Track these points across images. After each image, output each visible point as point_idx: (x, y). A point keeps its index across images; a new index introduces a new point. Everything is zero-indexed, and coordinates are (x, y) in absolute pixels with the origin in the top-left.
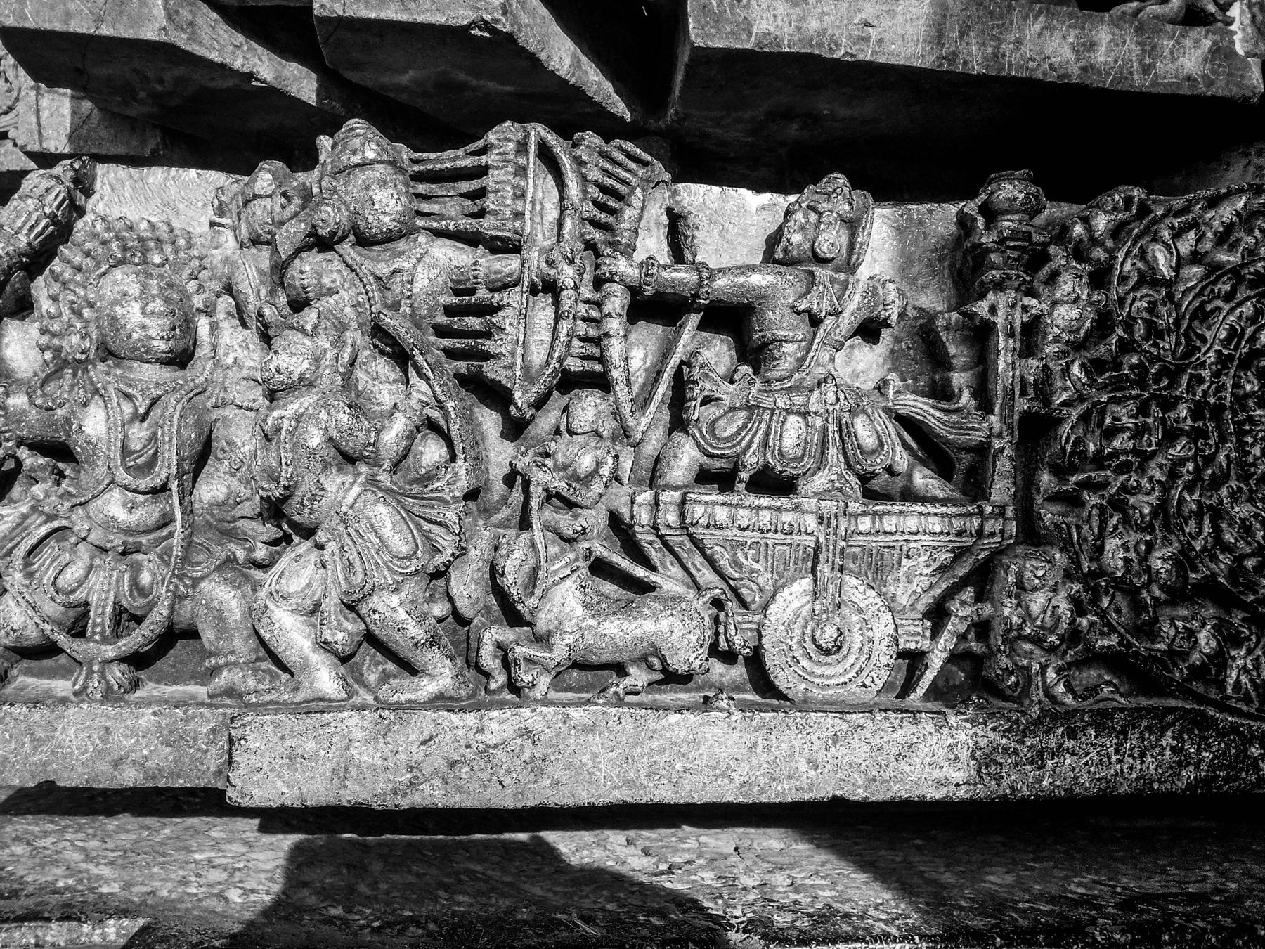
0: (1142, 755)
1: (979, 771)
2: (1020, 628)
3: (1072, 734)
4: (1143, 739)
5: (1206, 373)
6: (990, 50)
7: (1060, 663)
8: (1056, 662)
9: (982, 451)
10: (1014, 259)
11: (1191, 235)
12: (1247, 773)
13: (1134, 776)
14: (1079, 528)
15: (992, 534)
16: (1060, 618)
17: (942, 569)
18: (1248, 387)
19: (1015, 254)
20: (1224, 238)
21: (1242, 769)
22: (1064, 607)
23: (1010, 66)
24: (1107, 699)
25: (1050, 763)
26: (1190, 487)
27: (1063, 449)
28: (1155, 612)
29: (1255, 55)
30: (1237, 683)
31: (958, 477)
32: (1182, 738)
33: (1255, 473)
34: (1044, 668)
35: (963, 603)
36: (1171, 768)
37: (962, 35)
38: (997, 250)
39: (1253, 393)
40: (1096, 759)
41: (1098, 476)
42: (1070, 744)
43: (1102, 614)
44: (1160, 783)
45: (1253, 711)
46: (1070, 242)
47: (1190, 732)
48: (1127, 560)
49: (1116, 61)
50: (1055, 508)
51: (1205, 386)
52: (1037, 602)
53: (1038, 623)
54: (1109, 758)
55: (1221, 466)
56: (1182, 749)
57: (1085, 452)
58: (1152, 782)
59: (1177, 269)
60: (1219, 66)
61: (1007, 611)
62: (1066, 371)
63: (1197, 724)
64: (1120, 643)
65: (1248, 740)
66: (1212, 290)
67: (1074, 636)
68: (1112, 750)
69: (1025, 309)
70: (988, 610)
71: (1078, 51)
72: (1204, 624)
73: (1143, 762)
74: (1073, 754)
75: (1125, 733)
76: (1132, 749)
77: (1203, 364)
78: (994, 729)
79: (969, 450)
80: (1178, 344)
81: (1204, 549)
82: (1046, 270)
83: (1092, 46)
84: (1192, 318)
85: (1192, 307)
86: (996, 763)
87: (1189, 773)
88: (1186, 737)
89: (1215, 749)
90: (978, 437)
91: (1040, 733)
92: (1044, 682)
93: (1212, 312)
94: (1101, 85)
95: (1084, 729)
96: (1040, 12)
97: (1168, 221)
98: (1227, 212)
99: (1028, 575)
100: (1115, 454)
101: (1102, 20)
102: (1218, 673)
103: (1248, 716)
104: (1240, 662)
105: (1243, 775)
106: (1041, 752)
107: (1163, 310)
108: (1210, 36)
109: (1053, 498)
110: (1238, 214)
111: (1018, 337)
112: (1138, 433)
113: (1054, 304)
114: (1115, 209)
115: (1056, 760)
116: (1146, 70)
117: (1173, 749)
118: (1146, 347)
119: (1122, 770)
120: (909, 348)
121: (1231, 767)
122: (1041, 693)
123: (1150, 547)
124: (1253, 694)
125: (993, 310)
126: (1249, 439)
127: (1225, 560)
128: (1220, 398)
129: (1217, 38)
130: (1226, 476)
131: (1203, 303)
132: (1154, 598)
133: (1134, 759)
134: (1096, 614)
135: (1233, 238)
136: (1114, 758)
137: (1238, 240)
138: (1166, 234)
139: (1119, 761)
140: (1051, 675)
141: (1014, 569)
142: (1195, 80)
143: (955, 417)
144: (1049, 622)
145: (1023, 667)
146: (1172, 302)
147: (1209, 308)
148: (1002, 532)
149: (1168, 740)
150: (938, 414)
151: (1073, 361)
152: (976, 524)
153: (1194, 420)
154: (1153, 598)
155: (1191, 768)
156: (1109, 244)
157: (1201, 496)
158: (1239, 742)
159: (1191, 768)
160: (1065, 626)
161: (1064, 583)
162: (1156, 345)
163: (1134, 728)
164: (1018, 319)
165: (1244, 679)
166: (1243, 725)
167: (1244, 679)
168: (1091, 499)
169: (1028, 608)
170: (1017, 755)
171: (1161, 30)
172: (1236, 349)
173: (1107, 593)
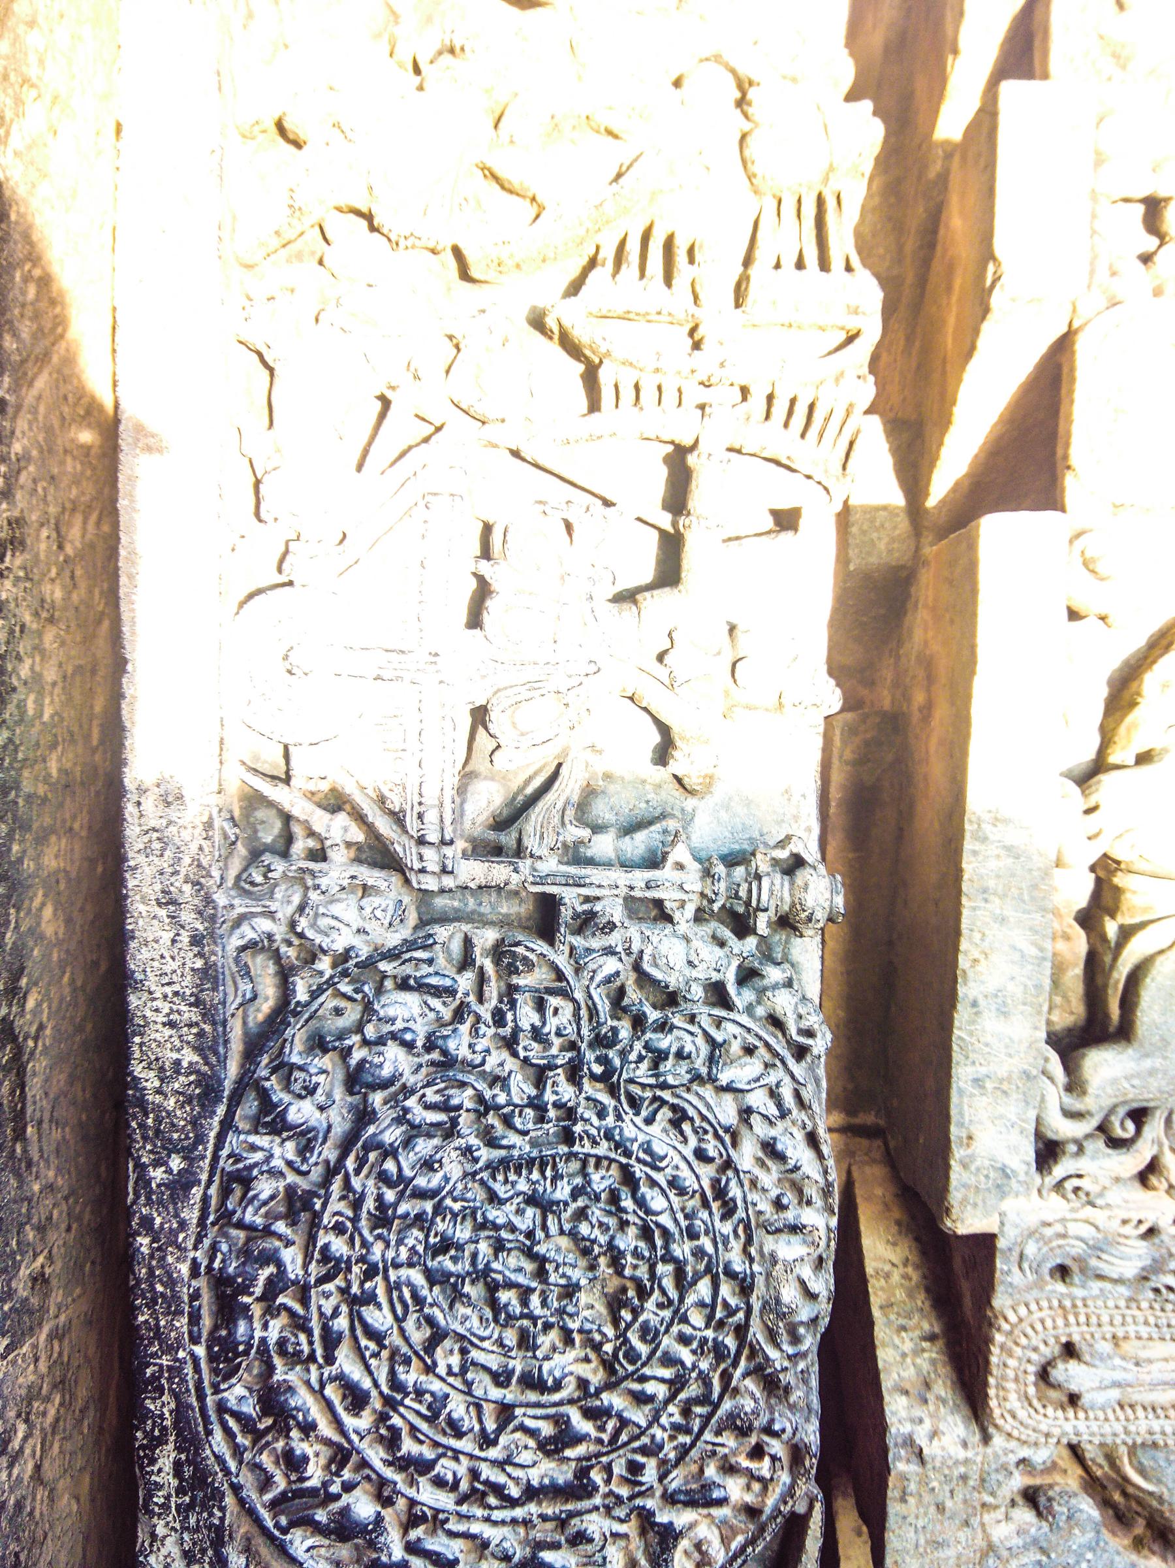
0: (171, 1024)
1: (154, 830)
2: (317, 887)
3: (196, 940)
4: (190, 1026)
5: (610, 1120)
6: (991, 883)
7: (278, 937)
8: (279, 931)
9: (519, 851)
10: (737, 892)
11: (773, 1111)
12: (151, 1152)
13: (148, 1013)
14: (430, 962)
15: (421, 858)
16: (327, 935)
17: (382, 800)
18: (595, 1177)
19: (743, 893)
20: (770, 1149)
21: (155, 1146)
22: (339, 946)
23: (974, 909)
24: (236, 990)
25: (162, 913)
26: (480, 1098)
27: (518, 944)
28: (335, 1049)
29: (1002, 1223)
30: (253, 1148)
31: (492, 835)
32: (191, 1073)
33: (495, 1179)
34: (271, 915)
35: (346, 830)
36: (157, 1059)
37: (1008, 849)
38: (748, 874)
39: (589, 1183)
40: (167, 969)
41: (493, 990)
42: (185, 938)
43: (330, 983)
44: (141, 1045)
45: (221, 1163)
46: (761, 963)
47: (198, 1083)
48: (393, 1020)
49: (987, 1045)
50: (456, 946)
51: (595, 1121)
52: (347, 909)
53: (321, 910)
54: (169, 984)
55: (503, 1137)
56: (178, 1072)
57: (517, 972)
58: (142, 1035)
59: (729, 1089)
60: (987, 1177)
61: (334, 874)
62: (609, 951)
63: (208, 1090)
64: (298, 1003)
65: (189, 1155)
66: (706, 1132)
67: (311, 955)
68: (176, 988)
69: (682, 904)
70: (339, 856)
71: (996, 996)
72: (322, 1109)
73: (164, 1024)
74: (174, 941)
75: (196, 1004)
76: (179, 1012)
77: (619, 1117)
78: (201, 849)
79: (519, 841)
80: (643, 1086)
81: (406, 1111)
82: (726, 933)
83: (1003, 1013)
84: (674, 1108)
85: (686, 1106)
86: (163, 850)
87: (151, 1081)
88: (192, 1078)
89: (178, 1113)
90: (531, 843)
91: (196, 902)
92: (254, 915)
93: (682, 1133)
94: (956, 1023)
95: (200, 955)
96: (1041, 949)
97: (787, 1079)
98: (798, 1152)
99: (376, 901)
100: (513, 1004)
101: (1036, 1028)
102: (266, 1125)
103: (216, 1158)
104: (277, 1151)
105: (149, 1147)
106: (173, 902)
107: (684, 1066)
108: (1024, 1167)
109: (468, 943)
110: (796, 1168)
111: (650, 894)
112: (537, 1034)
113: (687, 940)
114: (800, 1017)
115: (167, 921)
116: (978, 1083)
117: (177, 1063)
118: (638, 1046)
119: (154, 999)
120: (647, 802)
121: (158, 1132)
122: (242, 910)
123: (409, 1046)
124: (240, 1166)
125: (680, 866)
126: (535, 1175)
127: (392, 1135)
128: (581, 1139)
129: (1022, 1177)
130: (492, 1142)
131: (692, 1120)
132: (351, 1048)
133: (168, 1015)
134: (332, 977)
135: (769, 1163)
136: (168, 990)
137: (768, 1170)
138: (772, 1078)
139: (165, 996)
140: (265, 925)
141: (383, 885)
142: (968, 1146)
143: (556, 820)
144: (323, 922)
145: (272, 893)
146: (691, 1081)
147: (686, 1127)
148: (423, 871)
149: (189, 1057)
150: (560, 805)
151: (620, 960)
152: (433, 837)
153: (555, 1105)
154: (351, 1048)
155: (157, 1084)
156: (760, 1011)
157: (468, 1110)
158: (186, 1143)
159: (157, 1084)
160: (317, 941)
161: (367, 942)
162: (641, 1058)
163: (204, 1015)
164: (669, 896)
165: (258, 1156)
166: (206, 1149)
167: (258, 1156)
168: (465, 982)
169: (338, 900)
170: (173, 874)
171: (1027, 1103)
172: (638, 1160)
173: (356, 991)
